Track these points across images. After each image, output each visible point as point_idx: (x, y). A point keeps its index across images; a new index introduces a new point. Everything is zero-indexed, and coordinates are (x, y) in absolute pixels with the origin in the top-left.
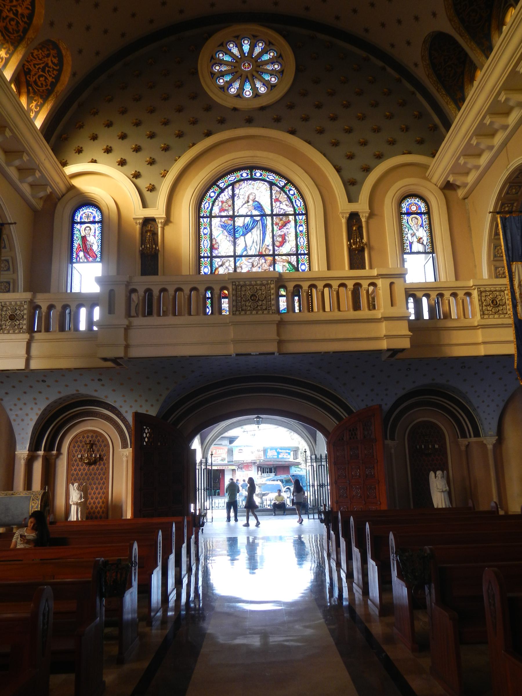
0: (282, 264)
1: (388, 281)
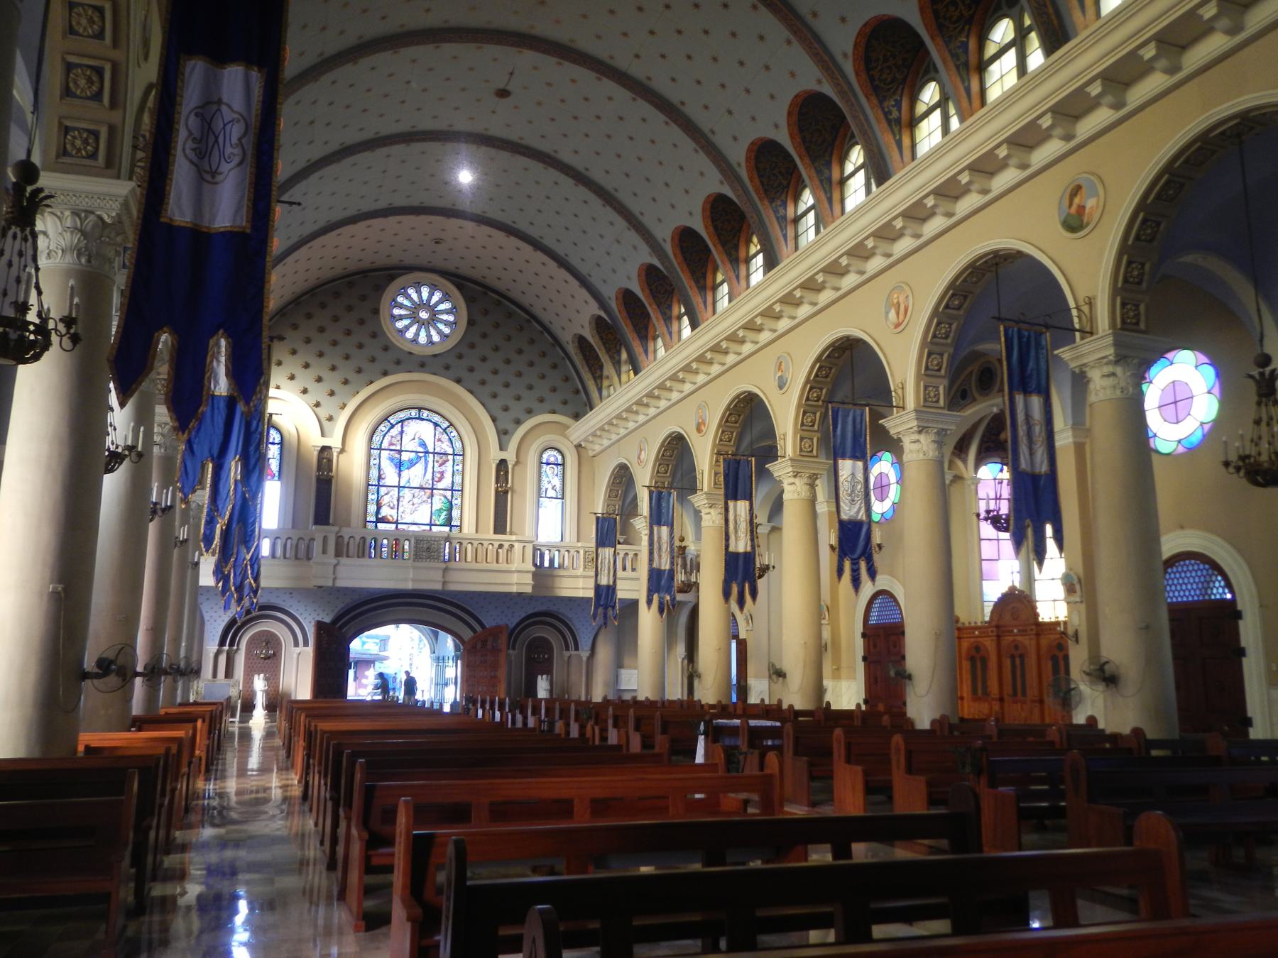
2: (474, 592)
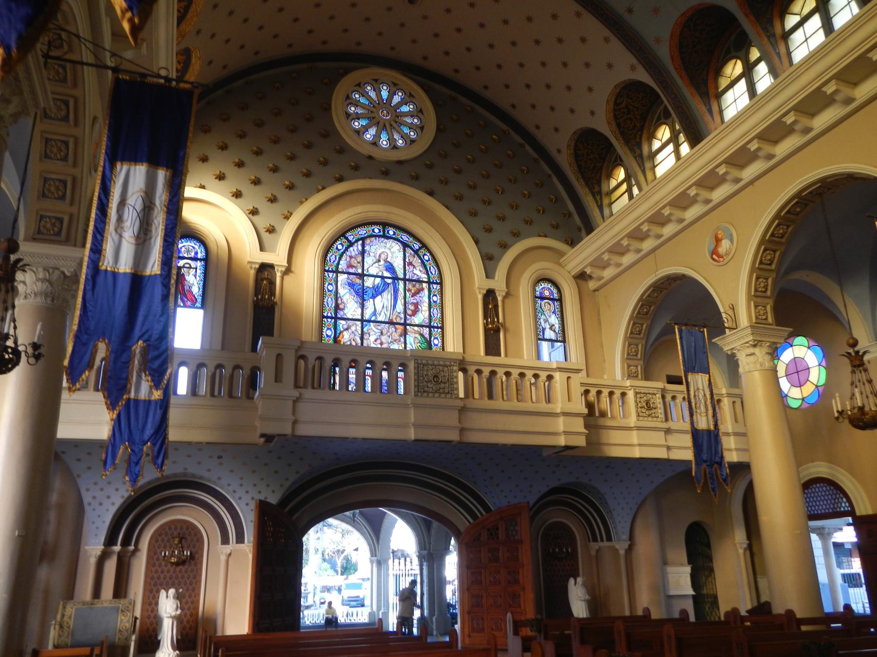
0: (413, 335)
1: (566, 375)
2: (504, 446)
